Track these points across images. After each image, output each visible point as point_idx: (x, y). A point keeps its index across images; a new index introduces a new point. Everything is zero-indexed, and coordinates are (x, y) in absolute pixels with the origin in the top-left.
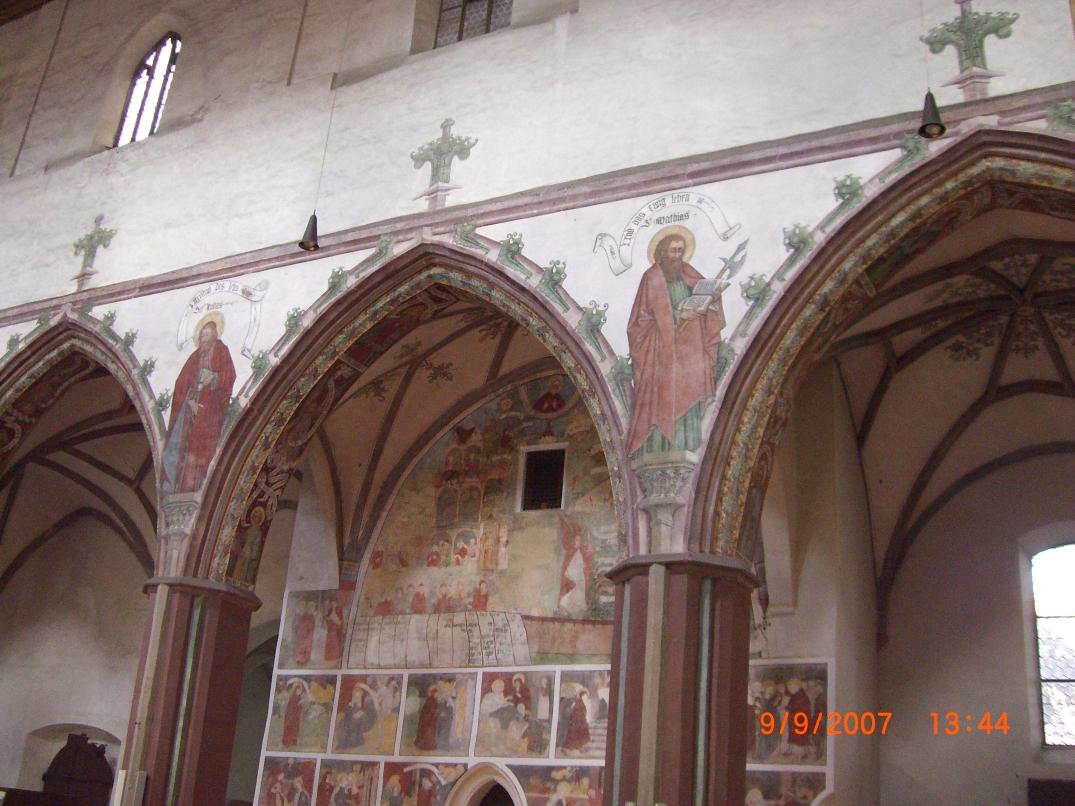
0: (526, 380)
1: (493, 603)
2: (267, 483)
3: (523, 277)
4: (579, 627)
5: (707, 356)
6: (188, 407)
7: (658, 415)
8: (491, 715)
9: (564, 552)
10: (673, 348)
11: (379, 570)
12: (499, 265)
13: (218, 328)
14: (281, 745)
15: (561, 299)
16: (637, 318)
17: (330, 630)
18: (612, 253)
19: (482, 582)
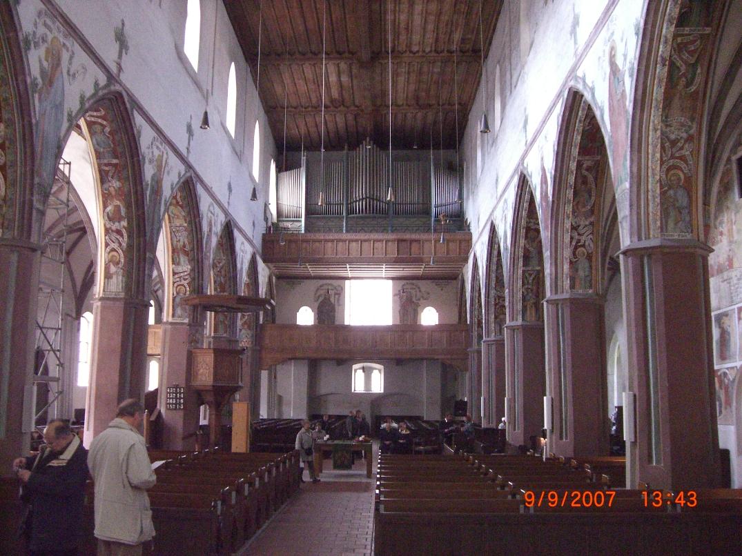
2: (579, 234)
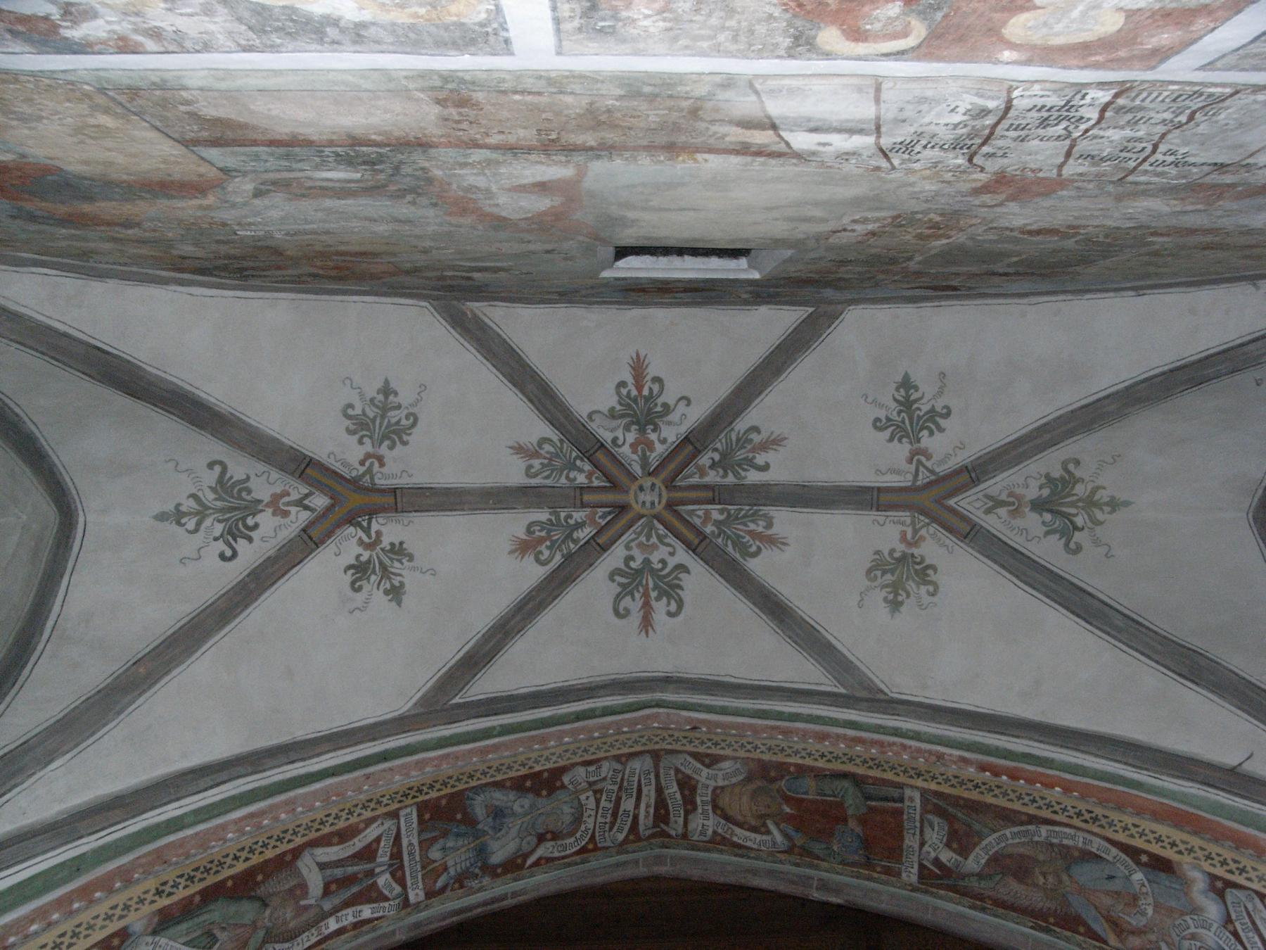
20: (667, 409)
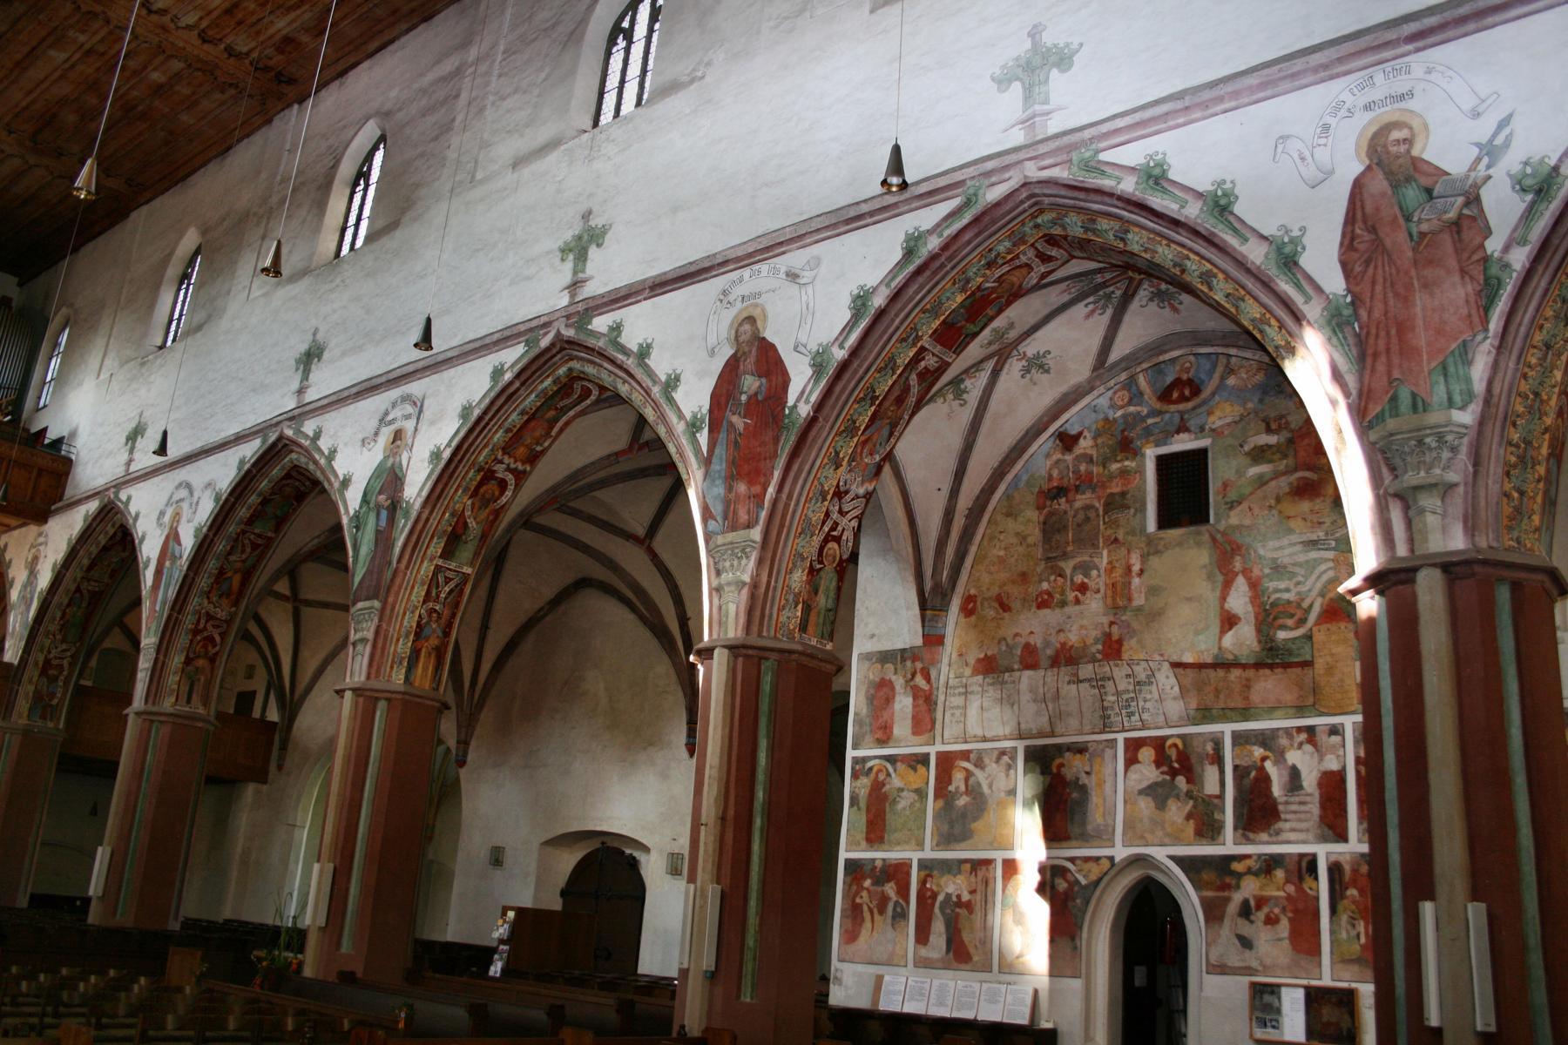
0: (1145, 366)
1: (1130, 649)
2: (840, 512)
3: (1175, 207)
4: (1251, 673)
5: (1467, 279)
6: (731, 424)
7: (1400, 366)
8: (1141, 792)
9: (1220, 578)
10: (1413, 273)
11: (973, 618)
12: (1139, 195)
13: (759, 324)
14: (864, 843)
15: (1235, 230)
16: (1352, 239)
17: (915, 698)
18: (1303, 159)
19: (1112, 623)
20: (1151, 300)
